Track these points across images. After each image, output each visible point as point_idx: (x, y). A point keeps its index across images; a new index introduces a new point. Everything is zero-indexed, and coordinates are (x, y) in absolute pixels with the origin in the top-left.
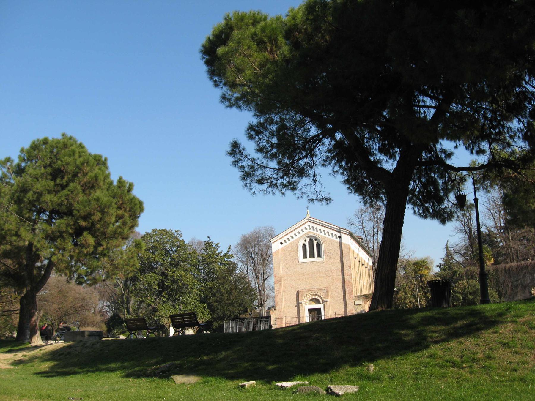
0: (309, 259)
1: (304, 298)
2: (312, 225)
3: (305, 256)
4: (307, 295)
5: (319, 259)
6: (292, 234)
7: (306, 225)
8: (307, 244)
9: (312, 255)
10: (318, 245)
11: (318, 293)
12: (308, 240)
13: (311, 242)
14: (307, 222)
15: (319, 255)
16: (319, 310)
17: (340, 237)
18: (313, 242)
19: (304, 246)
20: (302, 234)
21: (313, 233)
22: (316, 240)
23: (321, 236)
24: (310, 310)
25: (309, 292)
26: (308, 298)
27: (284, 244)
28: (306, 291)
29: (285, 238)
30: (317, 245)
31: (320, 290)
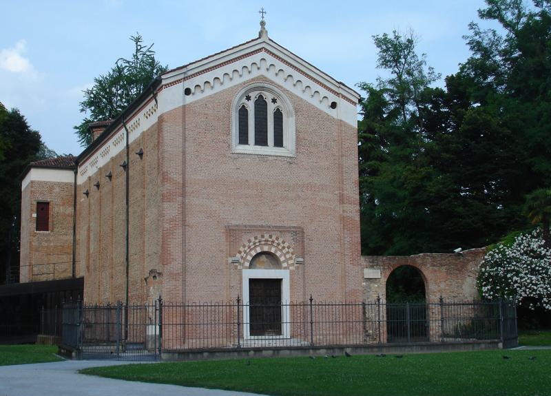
0: (251, 148)
1: (242, 249)
2: (270, 60)
3: (243, 140)
4: (249, 241)
7: (256, 58)
9: (261, 140)
10: (278, 116)
11: (277, 239)
12: (254, 95)
13: (261, 105)
14: (260, 50)
15: (279, 142)
16: (278, 282)
17: (334, 105)
18: (266, 103)
19: (243, 112)
20: (247, 77)
21: (272, 83)
22: (274, 101)
24: (253, 282)
25: (256, 234)
26: (251, 250)
28: (250, 232)
30: (275, 114)
31: (282, 230)
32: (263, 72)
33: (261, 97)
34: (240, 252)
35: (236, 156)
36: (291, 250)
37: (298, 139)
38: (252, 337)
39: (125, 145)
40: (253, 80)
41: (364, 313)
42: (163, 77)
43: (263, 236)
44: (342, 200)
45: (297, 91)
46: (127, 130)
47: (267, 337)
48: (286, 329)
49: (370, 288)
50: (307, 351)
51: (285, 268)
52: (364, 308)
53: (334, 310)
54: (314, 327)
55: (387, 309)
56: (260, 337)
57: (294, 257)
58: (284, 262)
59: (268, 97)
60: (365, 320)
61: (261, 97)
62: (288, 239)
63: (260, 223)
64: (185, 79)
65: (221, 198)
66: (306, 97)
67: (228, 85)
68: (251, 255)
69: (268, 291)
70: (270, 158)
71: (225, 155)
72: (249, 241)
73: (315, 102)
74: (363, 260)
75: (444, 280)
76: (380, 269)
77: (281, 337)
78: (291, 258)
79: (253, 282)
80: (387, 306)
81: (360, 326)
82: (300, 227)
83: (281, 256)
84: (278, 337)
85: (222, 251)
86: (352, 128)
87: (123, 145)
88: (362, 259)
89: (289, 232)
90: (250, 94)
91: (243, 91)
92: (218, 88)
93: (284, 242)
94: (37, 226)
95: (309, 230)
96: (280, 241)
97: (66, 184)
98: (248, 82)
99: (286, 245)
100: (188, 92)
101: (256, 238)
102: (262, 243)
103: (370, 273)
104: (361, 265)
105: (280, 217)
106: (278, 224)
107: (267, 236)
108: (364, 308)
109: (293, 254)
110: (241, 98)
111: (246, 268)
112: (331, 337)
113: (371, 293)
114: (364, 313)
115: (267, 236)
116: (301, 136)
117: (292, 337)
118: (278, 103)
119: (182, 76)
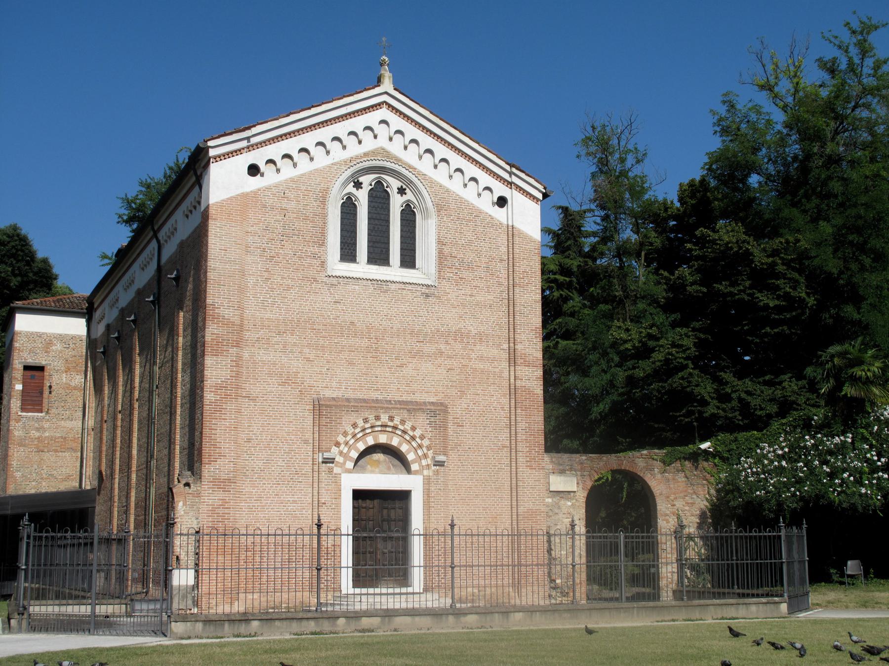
0: (362, 268)
1: (341, 439)
2: (396, 122)
3: (348, 253)
4: (355, 426)
5: (408, 275)
6: (308, 140)
7: (372, 118)
8: (362, 198)
9: (378, 256)
10: (408, 216)
11: (403, 422)
12: (367, 180)
15: (408, 260)
16: (403, 496)
17: (502, 202)
19: (349, 208)
20: (354, 149)
21: (398, 161)
22: (402, 191)
23: (432, 183)
24: (359, 495)
26: (357, 440)
27: (270, 177)
28: (356, 409)
29: (275, 151)
31: (412, 408)
32: (382, 142)
33: (379, 183)
34: (338, 444)
35: (335, 281)
36: (426, 442)
37: (441, 257)
38: (358, 591)
39: (155, 266)
40: (366, 154)
41: (549, 551)
42: (210, 143)
43: (378, 418)
44: (513, 359)
45: (440, 176)
46: (158, 242)
47: (384, 591)
48: (417, 576)
49: (559, 508)
50: (444, 617)
51: (416, 473)
52: (549, 542)
53: (499, 544)
54: (456, 575)
55: (588, 545)
56: (371, 591)
57: (430, 453)
58: (414, 461)
59: (393, 184)
60: (551, 561)
61: (379, 183)
62: (421, 425)
63: (374, 395)
64: (250, 148)
65: (306, 350)
66: (455, 185)
67: (321, 160)
68: (356, 449)
69: (385, 511)
70: (393, 286)
71: (315, 280)
72: (355, 426)
73: (470, 194)
74: (547, 460)
75: (682, 495)
76: (577, 475)
77: (410, 590)
78: (425, 456)
79: (359, 495)
80: (587, 538)
81: (542, 572)
82: (442, 404)
83: (409, 451)
84: (404, 590)
85: (306, 442)
86: (532, 240)
87: (153, 266)
88: (547, 458)
89: (423, 411)
90: (361, 179)
91: (349, 173)
92: (304, 165)
93: (413, 428)
94: (22, 404)
95: (457, 409)
96: (408, 426)
97: (73, 337)
98: (357, 157)
99: (417, 433)
100: (254, 170)
101: (366, 420)
102: (377, 429)
103: (559, 483)
104: (543, 468)
105: (408, 385)
106: (404, 398)
107: (384, 418)
108: (549, 542)
109: (429, 448)
110: (345, 184)
111: (349, 471)
112: (494, 590)
113: (561, 515)
114: (549, 551)
115: (384, 418)
116: (446, 250)
117: (426, 590)
118: (409, 196)
119: (244, 144)
